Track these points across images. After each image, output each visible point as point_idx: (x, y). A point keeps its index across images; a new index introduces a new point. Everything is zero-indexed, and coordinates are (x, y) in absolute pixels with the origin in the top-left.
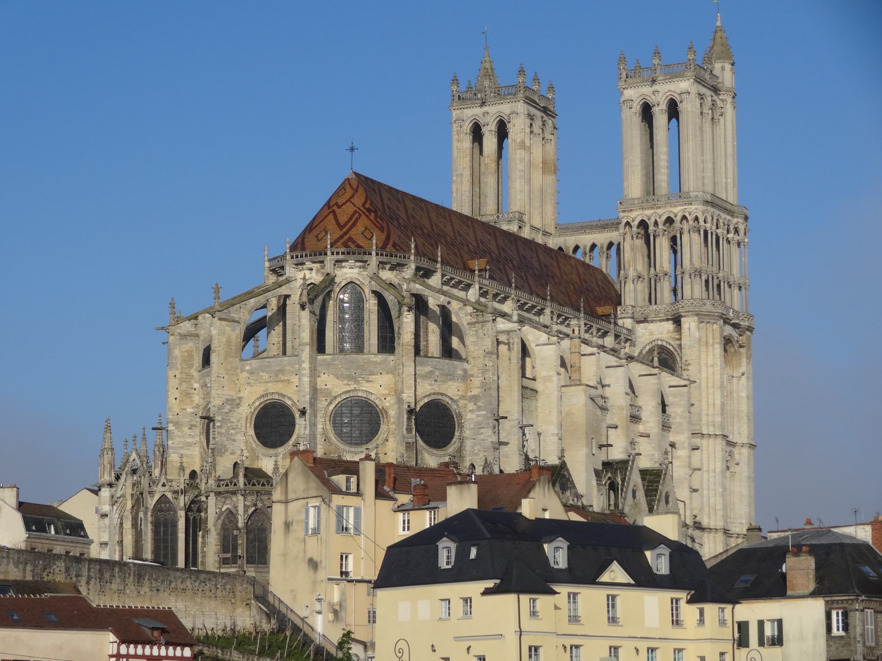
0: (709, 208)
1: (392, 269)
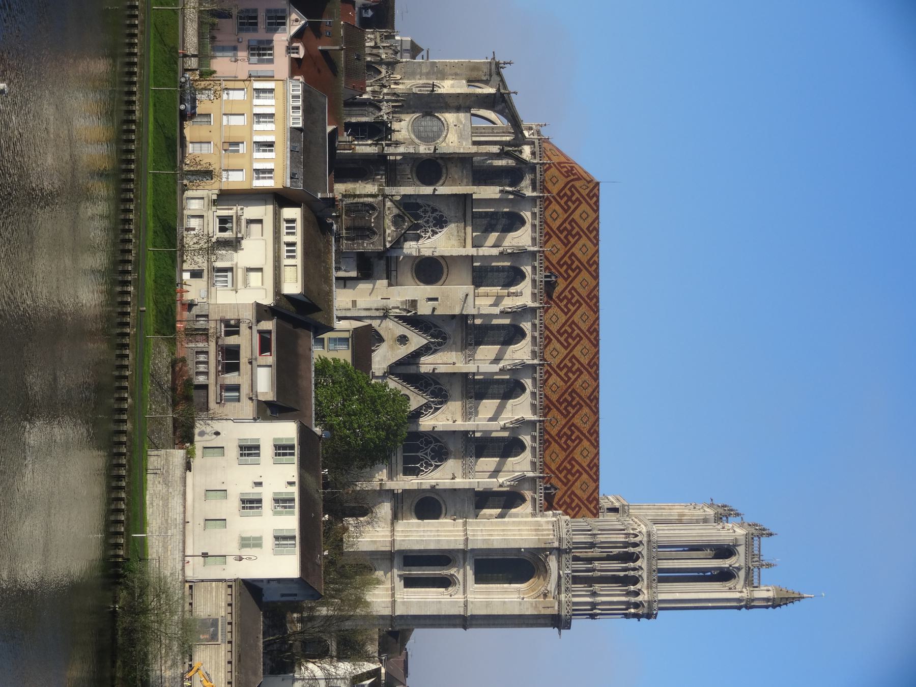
0: (645, 539)
1: (533, 153)
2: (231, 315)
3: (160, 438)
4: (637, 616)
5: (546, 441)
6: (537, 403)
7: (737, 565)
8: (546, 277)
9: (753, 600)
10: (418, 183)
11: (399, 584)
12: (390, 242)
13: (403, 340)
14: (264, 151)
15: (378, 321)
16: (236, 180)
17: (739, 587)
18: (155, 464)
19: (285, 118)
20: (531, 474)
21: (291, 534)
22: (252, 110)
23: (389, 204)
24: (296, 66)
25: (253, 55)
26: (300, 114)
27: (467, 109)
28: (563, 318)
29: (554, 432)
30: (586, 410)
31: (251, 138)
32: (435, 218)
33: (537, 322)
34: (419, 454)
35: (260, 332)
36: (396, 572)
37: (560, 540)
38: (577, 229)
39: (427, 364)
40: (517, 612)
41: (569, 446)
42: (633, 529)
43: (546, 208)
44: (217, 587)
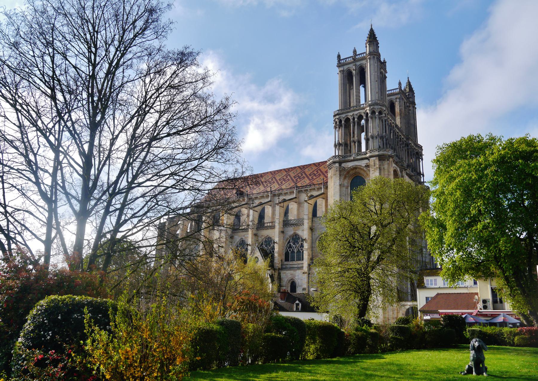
0: (337, 117)
30: (307, 170)
34: (296, 251)
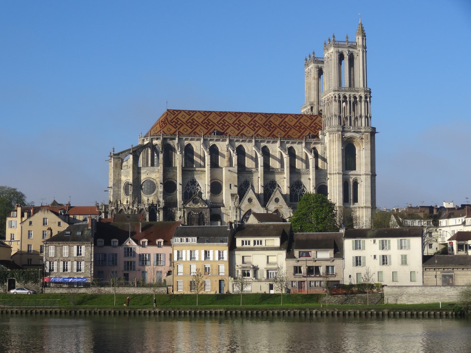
0: (337, 93)
1: (157, 139)
2: (292, 271)
3: (374, 299)
4: (370, 97)
5: (288, 136)
6: (272, 141)
7: (347, 52)
8: (214, 135)
9: (363, 45)
10: (175, 192)
11: (356, 205)
12: (205, 205)
13: (250, 200)
14: (209, 255)
15: (242, 211)
16: (224, 269)
17: (357, 51)
18: (392, 300)
19: (193, 245)
20: (304, 144)
21: (400, 241)
22: (188, 261)
23: (188, 206)
24: (152, 243)
25: (146, 264)
26: (190, 239)
27: (140, 169)
28: (231, 128)
29: (284, 134)
30: (272, 119)
31: (203, 261)
32: (192, 185)
33: (235, 139)
35: (300, 257)
36: (352, 206)
37: (338, 131)
38: (190, 120)
39: (260, 190)
40: (370, 152)
41: (289, 127)
42: (332, 97)
43: (183, 134)
44: (426, 275)
